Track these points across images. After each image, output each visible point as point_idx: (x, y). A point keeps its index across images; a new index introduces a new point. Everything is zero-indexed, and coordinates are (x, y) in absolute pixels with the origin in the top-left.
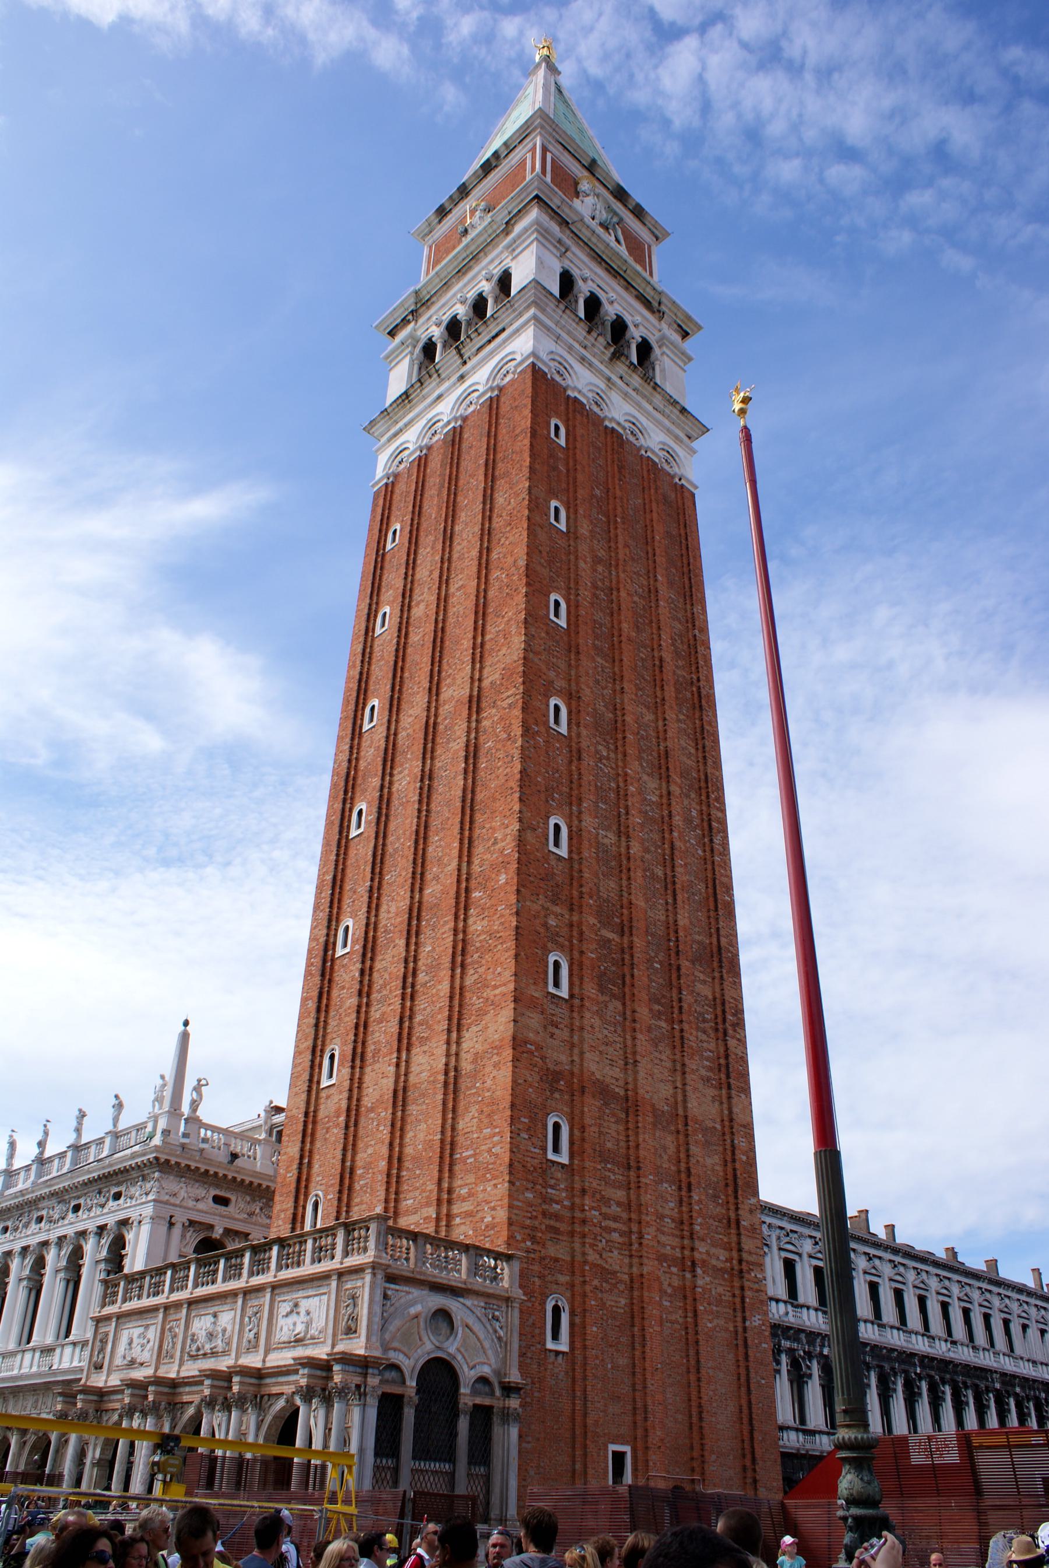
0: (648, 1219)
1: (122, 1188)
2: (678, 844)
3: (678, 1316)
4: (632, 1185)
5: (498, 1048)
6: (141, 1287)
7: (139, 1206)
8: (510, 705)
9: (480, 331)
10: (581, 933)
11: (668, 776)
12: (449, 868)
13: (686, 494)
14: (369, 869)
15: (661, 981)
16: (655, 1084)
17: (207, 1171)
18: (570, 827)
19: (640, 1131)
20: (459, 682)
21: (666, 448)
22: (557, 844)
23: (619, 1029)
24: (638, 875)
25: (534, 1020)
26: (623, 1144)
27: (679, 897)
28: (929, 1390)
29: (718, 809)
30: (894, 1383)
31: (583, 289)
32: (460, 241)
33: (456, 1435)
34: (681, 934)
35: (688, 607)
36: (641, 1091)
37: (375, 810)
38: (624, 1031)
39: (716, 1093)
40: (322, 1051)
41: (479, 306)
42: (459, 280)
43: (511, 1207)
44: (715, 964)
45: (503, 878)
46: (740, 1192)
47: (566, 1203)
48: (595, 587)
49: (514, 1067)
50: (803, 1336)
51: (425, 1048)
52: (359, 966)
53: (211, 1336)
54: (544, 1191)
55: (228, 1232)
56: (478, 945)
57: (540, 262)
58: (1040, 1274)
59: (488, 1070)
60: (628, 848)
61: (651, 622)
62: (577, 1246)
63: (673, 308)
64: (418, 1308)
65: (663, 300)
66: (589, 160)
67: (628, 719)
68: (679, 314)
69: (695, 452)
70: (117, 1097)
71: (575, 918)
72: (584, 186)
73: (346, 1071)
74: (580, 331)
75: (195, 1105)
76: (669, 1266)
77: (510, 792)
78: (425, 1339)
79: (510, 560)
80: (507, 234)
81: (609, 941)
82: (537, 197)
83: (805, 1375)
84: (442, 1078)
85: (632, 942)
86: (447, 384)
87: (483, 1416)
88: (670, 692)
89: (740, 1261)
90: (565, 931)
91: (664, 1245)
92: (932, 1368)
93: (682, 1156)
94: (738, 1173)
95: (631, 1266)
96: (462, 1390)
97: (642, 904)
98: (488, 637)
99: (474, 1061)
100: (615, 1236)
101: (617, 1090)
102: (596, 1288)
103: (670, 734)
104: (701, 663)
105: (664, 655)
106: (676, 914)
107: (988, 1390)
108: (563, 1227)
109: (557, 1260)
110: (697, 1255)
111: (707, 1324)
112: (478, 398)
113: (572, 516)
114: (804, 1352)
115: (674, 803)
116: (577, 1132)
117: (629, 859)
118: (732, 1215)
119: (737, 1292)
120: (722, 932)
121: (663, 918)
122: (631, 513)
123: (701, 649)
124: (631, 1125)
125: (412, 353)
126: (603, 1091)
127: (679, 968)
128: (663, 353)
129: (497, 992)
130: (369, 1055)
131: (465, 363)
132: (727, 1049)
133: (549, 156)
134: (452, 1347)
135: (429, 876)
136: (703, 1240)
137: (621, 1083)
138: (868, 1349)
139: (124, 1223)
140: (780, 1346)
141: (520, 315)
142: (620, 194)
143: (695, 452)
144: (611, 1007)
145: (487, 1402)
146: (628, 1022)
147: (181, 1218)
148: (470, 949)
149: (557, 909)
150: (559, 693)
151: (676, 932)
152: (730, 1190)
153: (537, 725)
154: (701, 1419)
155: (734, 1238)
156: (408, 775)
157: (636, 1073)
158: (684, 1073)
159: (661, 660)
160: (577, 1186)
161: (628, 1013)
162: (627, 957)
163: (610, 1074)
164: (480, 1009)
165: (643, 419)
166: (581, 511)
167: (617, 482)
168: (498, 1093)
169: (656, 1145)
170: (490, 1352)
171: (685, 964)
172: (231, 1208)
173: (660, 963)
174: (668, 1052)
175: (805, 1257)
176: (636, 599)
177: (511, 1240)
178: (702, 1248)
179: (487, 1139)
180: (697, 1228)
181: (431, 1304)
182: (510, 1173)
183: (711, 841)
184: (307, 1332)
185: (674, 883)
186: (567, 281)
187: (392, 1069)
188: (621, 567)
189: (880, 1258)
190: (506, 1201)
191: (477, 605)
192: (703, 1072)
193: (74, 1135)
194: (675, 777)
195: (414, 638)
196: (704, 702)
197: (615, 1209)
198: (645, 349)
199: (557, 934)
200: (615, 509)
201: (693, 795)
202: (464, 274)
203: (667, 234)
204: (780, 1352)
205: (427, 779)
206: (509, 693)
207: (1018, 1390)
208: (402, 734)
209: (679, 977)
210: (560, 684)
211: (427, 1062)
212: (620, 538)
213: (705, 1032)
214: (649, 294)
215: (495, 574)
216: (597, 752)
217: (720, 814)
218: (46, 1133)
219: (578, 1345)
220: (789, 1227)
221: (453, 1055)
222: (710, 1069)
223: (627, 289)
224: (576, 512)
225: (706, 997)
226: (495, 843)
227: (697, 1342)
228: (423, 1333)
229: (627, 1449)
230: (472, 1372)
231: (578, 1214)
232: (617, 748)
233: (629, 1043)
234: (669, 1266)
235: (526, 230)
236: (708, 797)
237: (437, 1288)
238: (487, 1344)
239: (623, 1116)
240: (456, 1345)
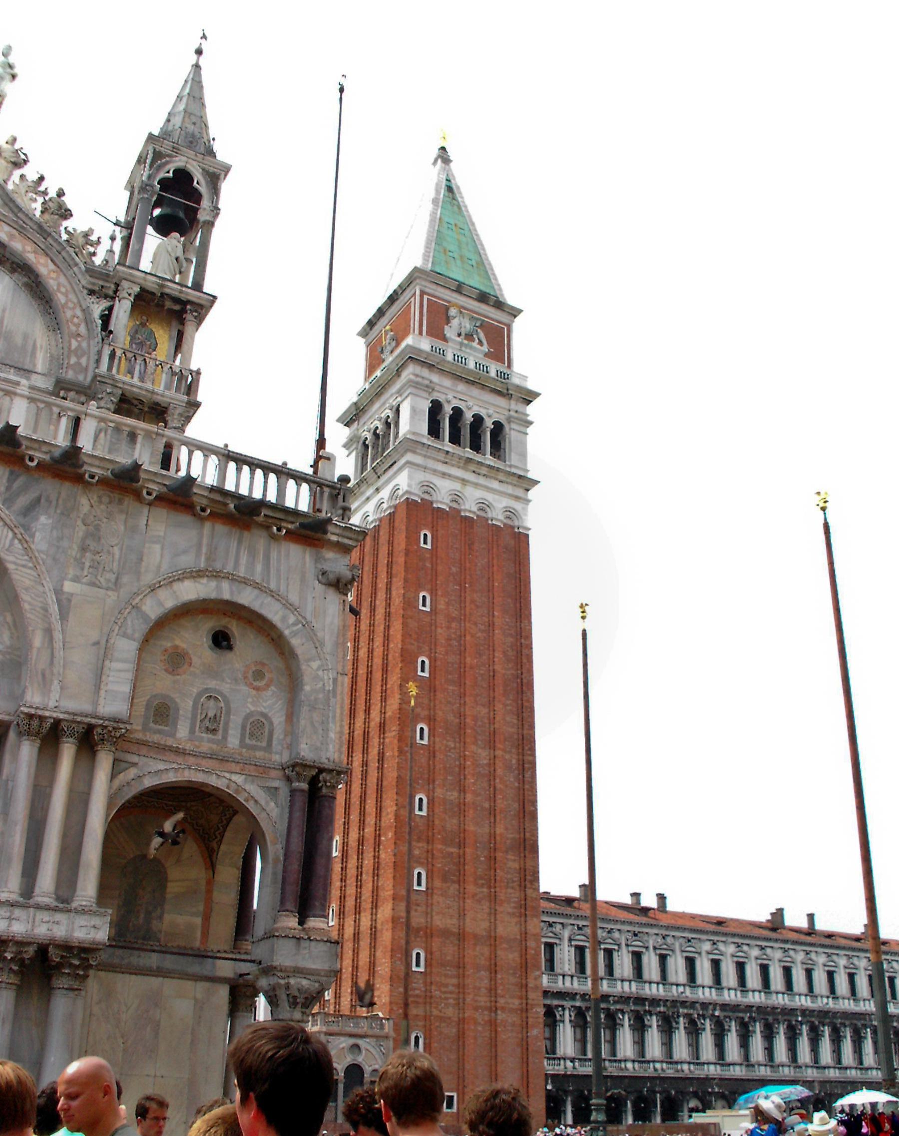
2: (499, 786)
3: (487, 1034)
10: (433, 855)
13: (522, 538)
16: (477, 921)
23: (457, 899)
24: (471, 813)
29: (529, 755)
31: (448, 410)
34: (498, 838)
35: (518, 624)
36: (467, 929)
39: (518, 919)
43: (391, 996)
44: (522, 848)
50: (698, 1005)
62: (428, 1008)
69: (529, 501)
71: (430, 847)
72: (453, 312)
82: (410, 357)
83: (699, 1029)
88: (499, 690)
89: (527, 1004)
92: (813, 1016)
93: (493, 956)
98: (388, 686)
100: (451, 1001)
103: (497, 719)
104: (525, 661)
105: (496, 667)
106: (495, 827)
108: (421, 1000)
109: (417, 1015)
110: (498, 1005)
111: (502, 1036)
114: (698, 1015)
116: (429, 956)
118: (524, 982)
119: (525, 1019)
120: (527, 830)
122: (478, 573)
123: (525, 651)
125: (357, 448)
126: (445, 933)
128: (511, 429)
133: (426, 297)
134: (360, 1059)
140: (678, 1012)
142: (483, 297)
143: (529, 501)
144: (452, 888)
146: (462, 896)
148: (381, 867)
149: (420, 845)
152: (523, 970)
155: (524, 993)
157: (464, 919)
158: (495, 914)
162: (462, 860)
163: (451, 923)
165: (490, 497)
169: (477, 954)
171: (499, 855)
173: (485, 857)
174: (488, 904)
175: (704, 954)
176: (479, 634)
178: (501, 1001)
180: (499, 991)
186: (436, 409)
192: (510, 910)
194: (498, 745)
196: (524, 688)
197: (451, 988)
198: (498, 428)
201: (514, 750)
203: (520, 311)
204: (678, 1017)
211: (365, 921)
213: (513, 888)
216: (447, 746)
217: (531, 758)
220: (690, 935)
221: (374, 920)
222: (515, 908)
223: (483, 389)
224: (436, 595)
225: (515, 869)
227: (496, 1045)
229: (455, 1094)
231: (428, 994)
237: (351, 1035)
238: (377, 1056)
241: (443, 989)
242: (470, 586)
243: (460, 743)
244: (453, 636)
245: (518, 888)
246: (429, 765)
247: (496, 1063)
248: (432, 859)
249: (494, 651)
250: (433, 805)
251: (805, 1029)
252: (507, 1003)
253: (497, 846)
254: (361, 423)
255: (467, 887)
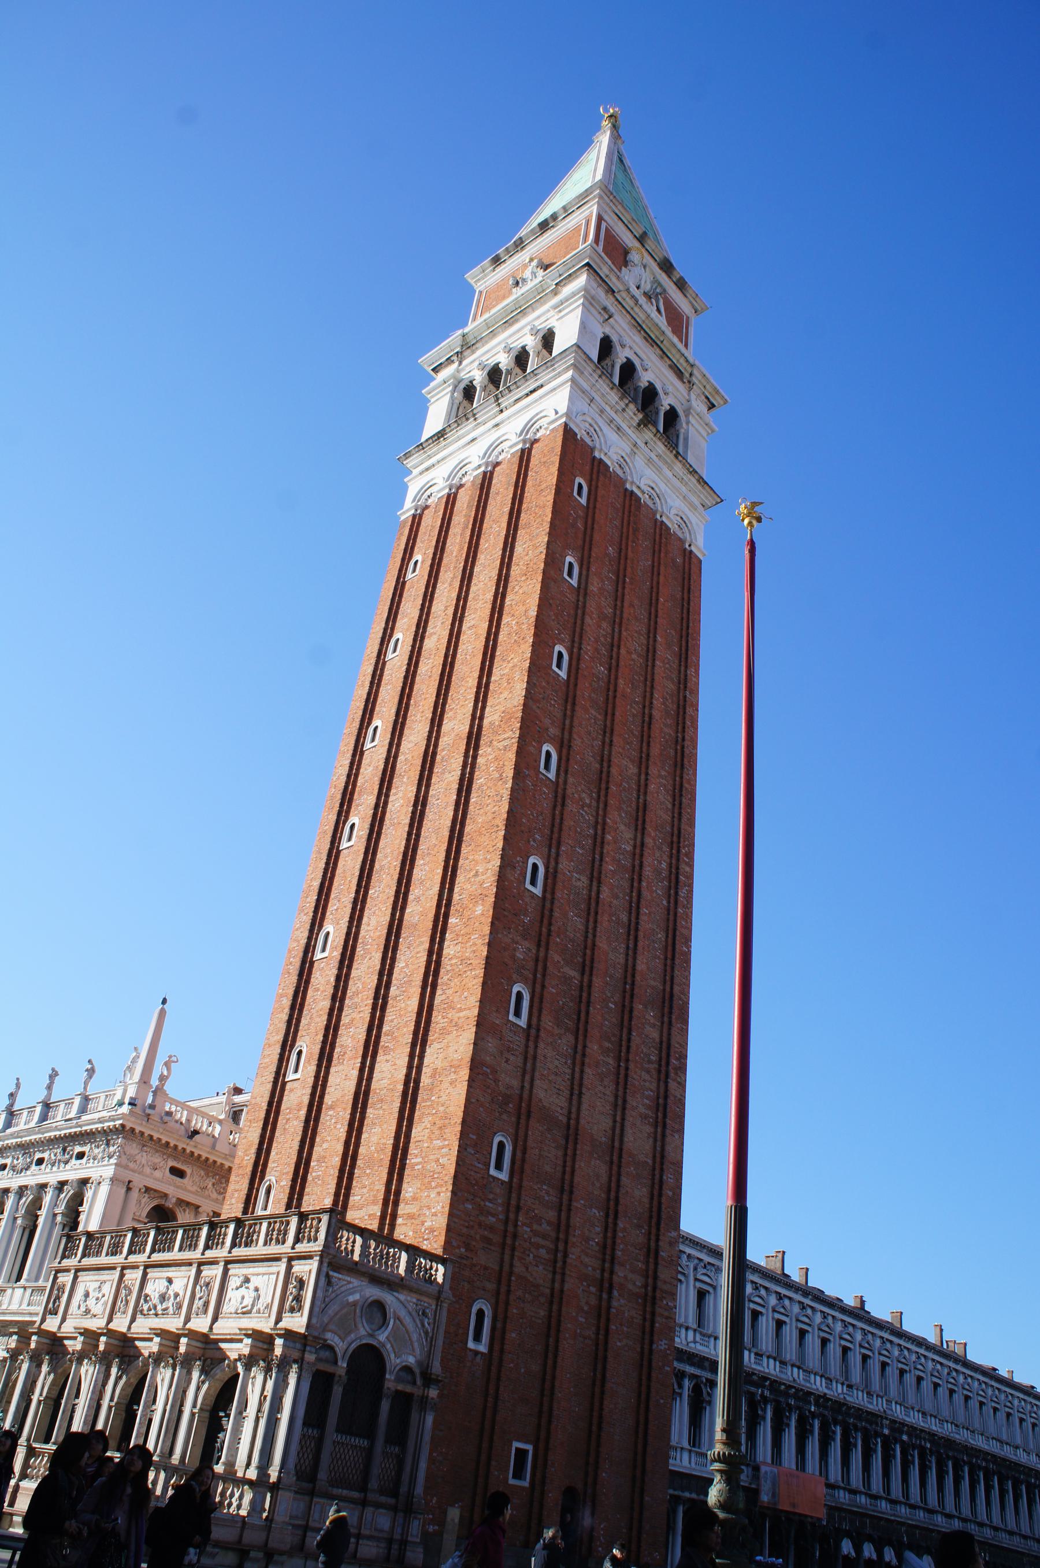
0: (574, 1240)
1: (86, 1149)
2: (645, 893)
3: (590, 1333)
4: (564, 1208)
5: (455, 1067)
6: (101, 1245)
7: (100, 1168)
8: (505, 747)
9: (519, 384)
10: (545, 968)
11: (644, 829)
12: (431, 892)
13: (694, 560)
14: (355, 881)
15: (614, 1020)
17: (168, 1143)
18: (547, 868)
19: (578, 1158)
20: (459, 717)
21: (680, 514)
22: (533, 882)
24: (604, 920)
25: (491, 1044)
26: (559, 1169)
27: (640, 944)
28: (820, 1428)
30: (789, 1418)
31: (621, 356)
32: (510, 293)
33: (378, 1415)
34: (638, 978)
36: (582, 1122)
37: (367, 826)
38: (574, 1063)
40: (292, 1046)
41: (521, 359)
42: (506, 329)
43: (451, 1215)
44: (666, 1010)
45: (479, 910)
46: (662, 1225)
47: (501, 1217)
48: (597, 641)
49: (469, 1086)
51: (388, 1057)
52: (335, 971)
53: (163, 1298)
54: (482, 1203)
55: (181, 1202)
56: (449, 968)
57: (583, 327)
58: (942, 1330)
59: (445, 1085)
60: (598, 892)
61: (646, 680)
63: (703, 381)
64: (357, 1296)
65: (695, 372)
66: (641, 232)
67: (614, 771)
68: (708, 387)
70: (90, 1061)
72: (634, 257)
73: (312, 1069)
74: (613, 397)
75: (163, 1079)
76: (589, 1286)
77: (495, 829)
78: (360, 1325)
79: (522, 609)
80: (556, 294)
81: (571, 978)
82: (588, 264)
84: (400, 1087)
85: (590, 981)
86: (481, 429)
87: (403, 1402)
89: (655, 1288)
90: (531, 965)
91: (586, 1266)
92: (826, 1408)
93: (613, 1185)
94: (663, 1206)
95: (553, 1281)
96: (387, 1376)
97: (605, 946)
99: (433, 1076)
100: (543, 1252)
101: (560, 1118)
102: (519, 1298)
104: (688, 723)
106: (635, 959)
107: (877, 1434)
109: (486, 1268)
112: (511, 447)
113: (584, 573)
115: (645, 854)
116: (519, 1154)
117: (597, 903)
121: (622, 961)
123: (689, 711)
124: (569, 1152)
125: (454, 390)
127: (631, 1011)
129: (461, 1014)
130: (335, 1056)
131: (502, 411)
132: (666, 1090)
133: (604, 225)
134: (382, 1337)
135: (411, 897)
136: (623, 1265)
137: (565, 1112)
138: (767, 1383)
139: (84, 1182)
141: (559, 374)
142: (667, 266)
145: (409, 1389)
146: (578, 1057)
147: (139, 1182)
150: (551, 740)
151: (633, 976)
153: (527, 768)
154: (600, 1428)
156: (402, 798)
158: (624, 1109)
159: (651, 716)
160: (513, 1202)
161: (580, 1047)
162: (585, 995)
164: (443, 1028)
166: (593, 569)
167: (630, 543)
168: (451, 1109)
169: (591, 1171)
170: (416, 1345)
171: (638, 1007)
172: (185, 1181)
173: (615, 1004)
174: (612, 1087)
176: (634, 656)
177: (447, 1245)
178: (620, 1273)
179: (436, 1150)
180: (619, 1253)
181: (368, 1295)
182: (454, 1184)
183: (677, 893)
184: (253, 1305)
185: (637, 930)
186: (606, 347)
187: (355, 1073)
188: (624, 625)
189: (790, 1298)
190: (447, 1209)
191: (486, 647)
192: (642, 1110)
193: (46, 1092)
194: (649, 829)
195: (422, 669)
197: (545, 1227)
198: (672, 416)
199: (523, 967)
200: (625, 570)
201: (666, 849)
202: (511, 325)
205: (420, 804)
206: (506, 736)
207: (905, 1437)
208: (401, 758)
209: (631, 1019)
210: (553, 731)
212: (627, 597)
213: (648, 1072)
214: (682, 365)
215: (506, 619)
216: (581, 799)
217: (687, 869)
218: (18, 1086)
219: (497, 1347)
222: (649, 1107)
225: (654, 1039)
226: (476, 875)
227: (605, 1358)
228: (358, 1319)
230: (398, 1361)
232: (599, 797)
233: (577, 1075)
234: (589, 1286)
235: (574, 294)
236: (678, 851)
237: (376, 1279)
238: (415, 1337)
239: (563, 1142)
240: (386, 1333)
241: (535, 1227)
242: (631, 583)
243: (598, 802)
244: (602, 639)
245: (654, 1074)
246: (554, 815)
247: (603, 1393)
248: (544, 975)
249: (652, 687)
250: (554, 884)
251: (817, 1424)
252: (625, 1277)
253: (636, 991)
254: (464, 363)
255: (589, 1044)
